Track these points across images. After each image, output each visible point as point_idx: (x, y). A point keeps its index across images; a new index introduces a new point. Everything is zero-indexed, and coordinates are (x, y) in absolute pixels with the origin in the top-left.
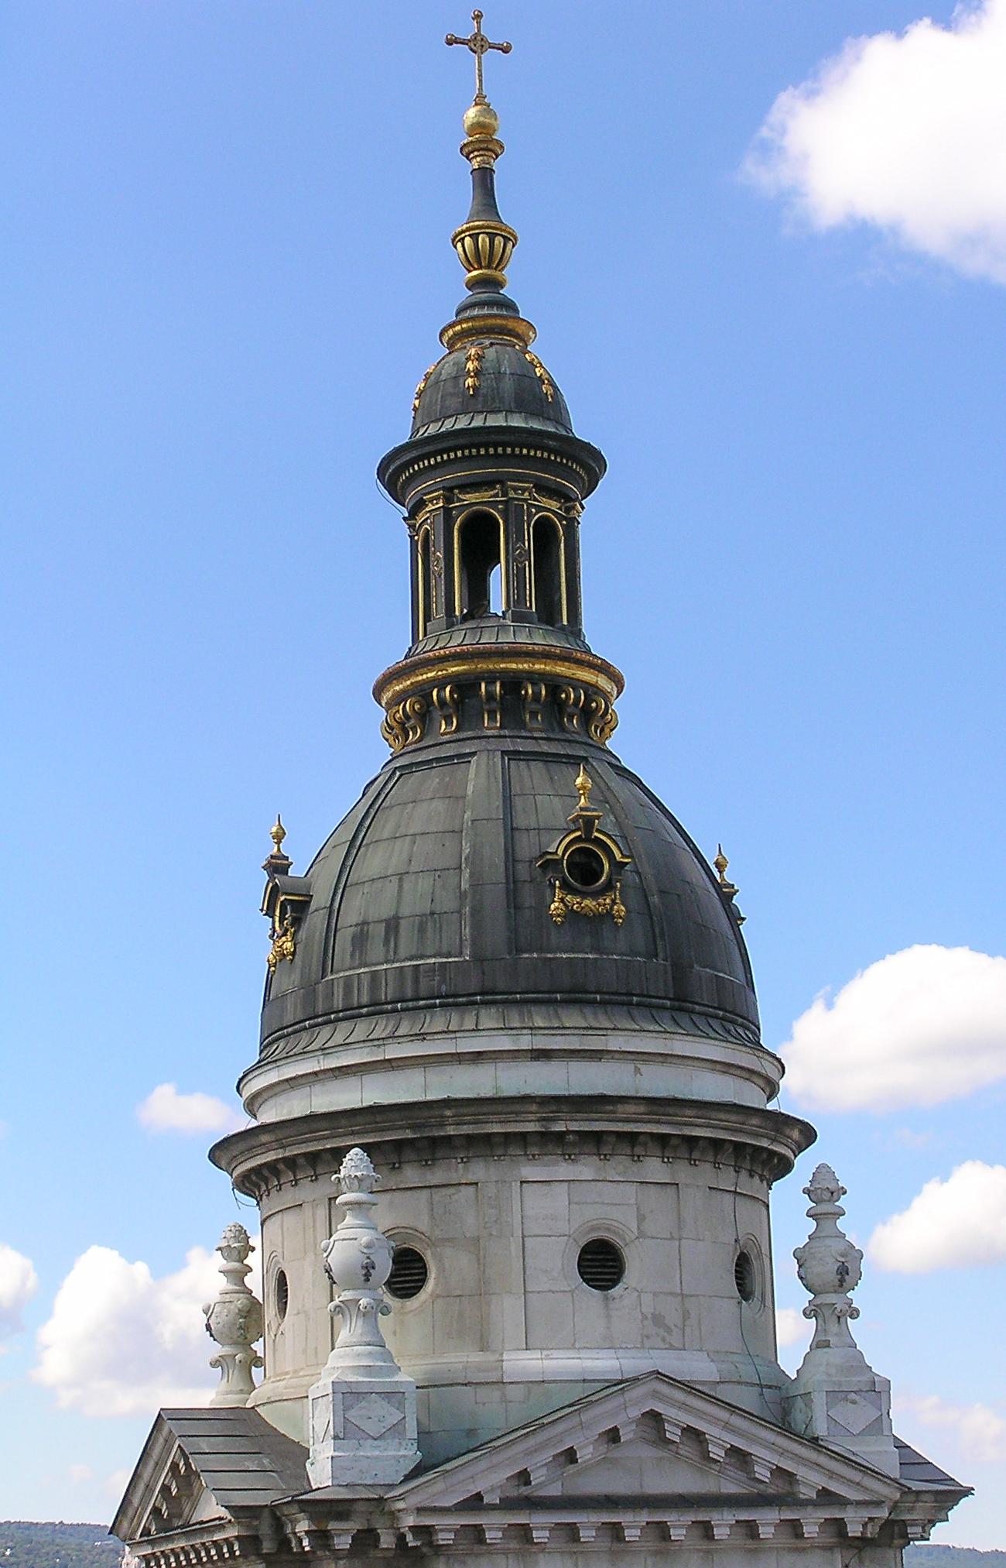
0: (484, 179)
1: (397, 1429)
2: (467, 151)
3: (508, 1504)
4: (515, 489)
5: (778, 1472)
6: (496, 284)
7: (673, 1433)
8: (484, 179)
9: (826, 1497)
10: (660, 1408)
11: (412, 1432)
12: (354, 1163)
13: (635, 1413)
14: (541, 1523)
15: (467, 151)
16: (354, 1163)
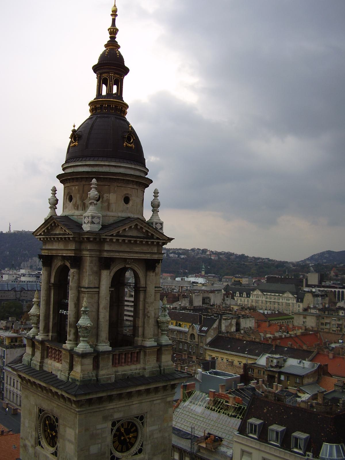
0: (114, 21)
1: (99, 223)
2: (112, 15)
3: (116, 236)
4: (111, 74)
5: (152, 234)
6: (115, 38)
7: (139, 227)
8: (114, 21)
9: (158, 238)
10: (138, 223)
11: (101, 224)
12: (94, 181)
13: (134, 224)
14: (121, 239)
15: (112, 15)
16: (94, 181)
